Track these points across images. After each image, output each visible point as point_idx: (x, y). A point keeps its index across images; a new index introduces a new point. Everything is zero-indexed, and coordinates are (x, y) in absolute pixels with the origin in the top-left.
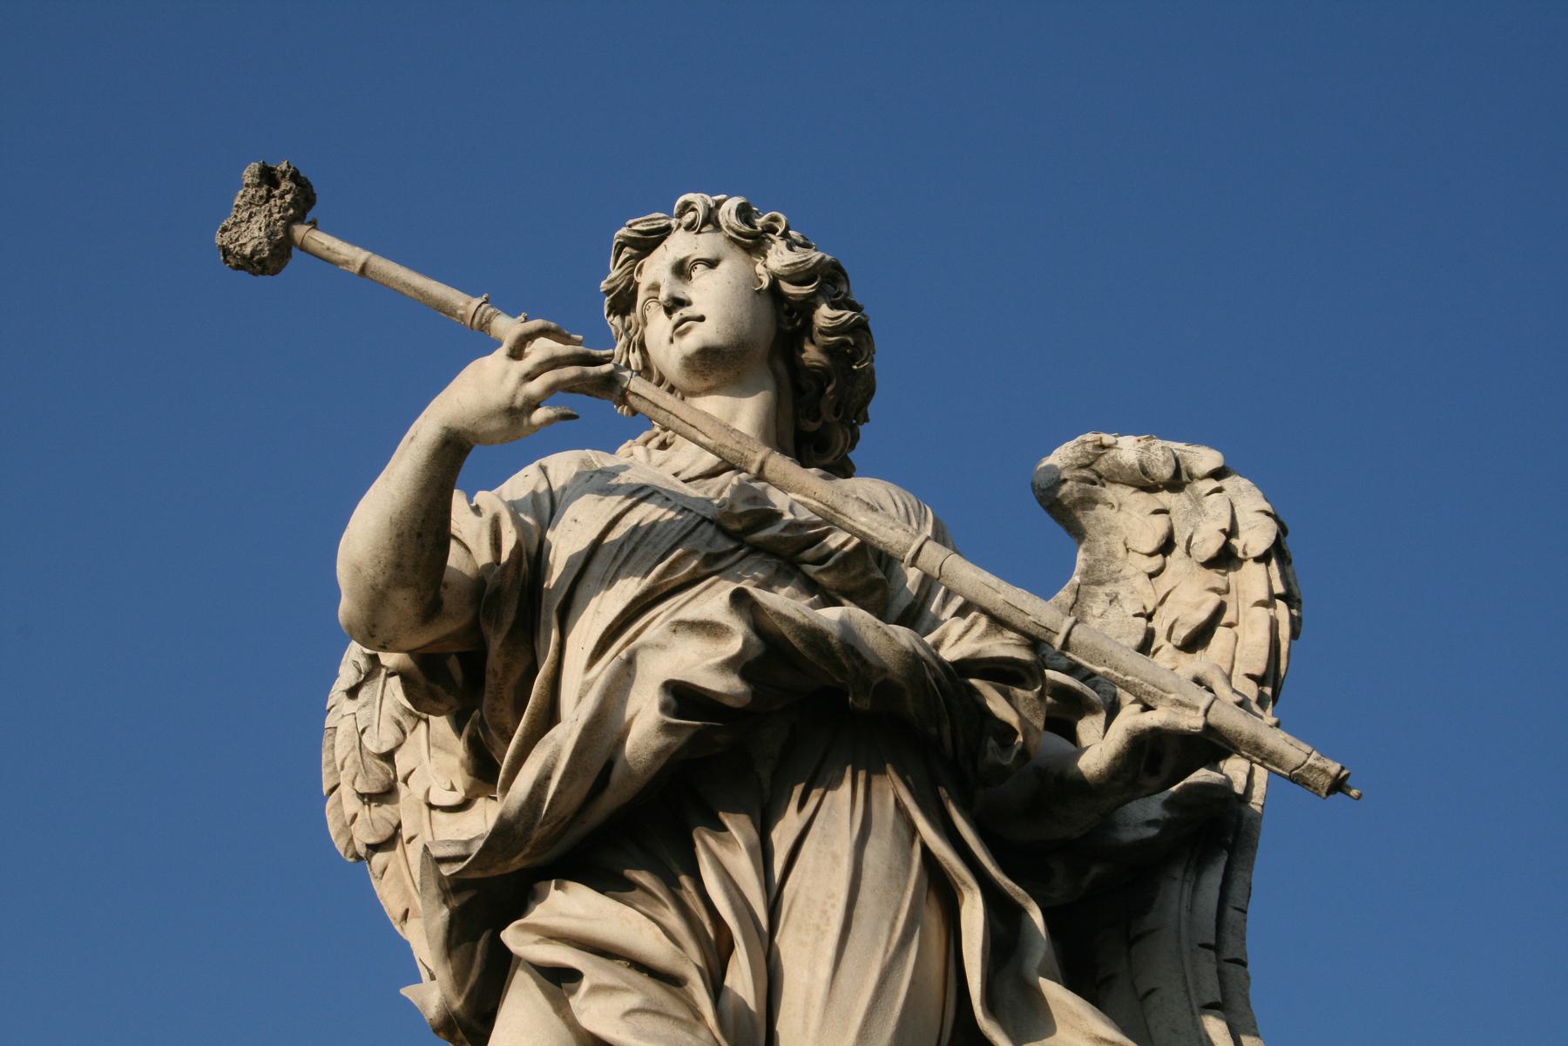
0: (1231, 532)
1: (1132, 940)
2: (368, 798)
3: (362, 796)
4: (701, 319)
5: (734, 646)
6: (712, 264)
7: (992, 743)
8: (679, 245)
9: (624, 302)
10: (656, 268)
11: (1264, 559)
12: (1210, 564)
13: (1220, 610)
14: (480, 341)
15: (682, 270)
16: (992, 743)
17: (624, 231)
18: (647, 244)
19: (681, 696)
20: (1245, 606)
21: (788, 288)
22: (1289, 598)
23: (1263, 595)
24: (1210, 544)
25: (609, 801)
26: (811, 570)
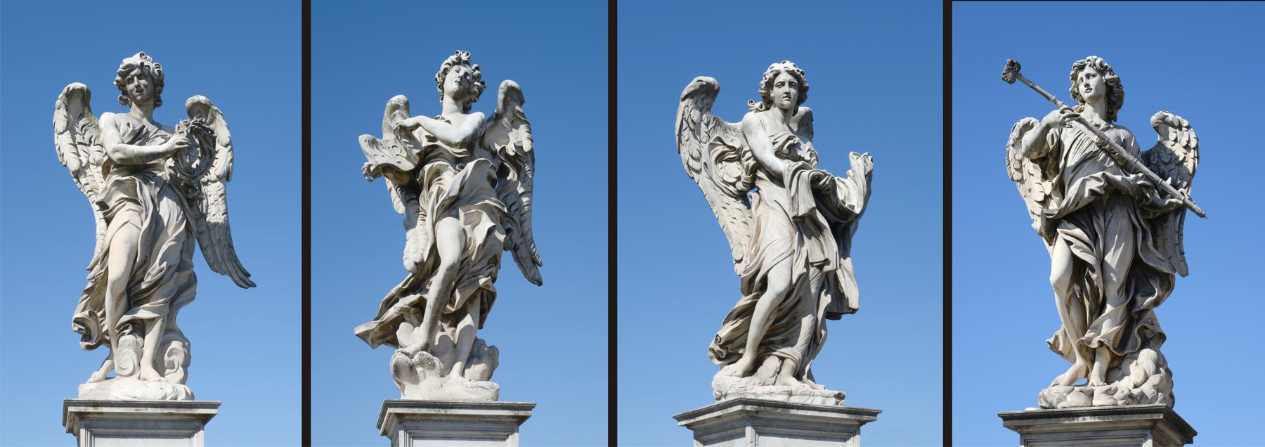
0: (1189, 142)
1: (1163, 229)
2: (1017, 169)
3: (1015, 169)
4: (1091, 89)
5: (1102, 183)
6: (1094, 76)
7: (1144, 200)
8: (1088, 70)
9: (1075, 77)
10: (1081, 74)
11: (1194, 149)
12: (1184, 147)
13: (1185, 158)
14: (1055, 105)
15: (1088, 76)
16: (1144, 200)
17: (1075, 64)
18: (1082, 68)
19: (1092, 192)
20: (1190, 158)
21: (1109, 83)
22: (1198, 157)
23: (1193, 156)
24: (1185, 143)
25: (1080, 206)
26: (1113, 155)
